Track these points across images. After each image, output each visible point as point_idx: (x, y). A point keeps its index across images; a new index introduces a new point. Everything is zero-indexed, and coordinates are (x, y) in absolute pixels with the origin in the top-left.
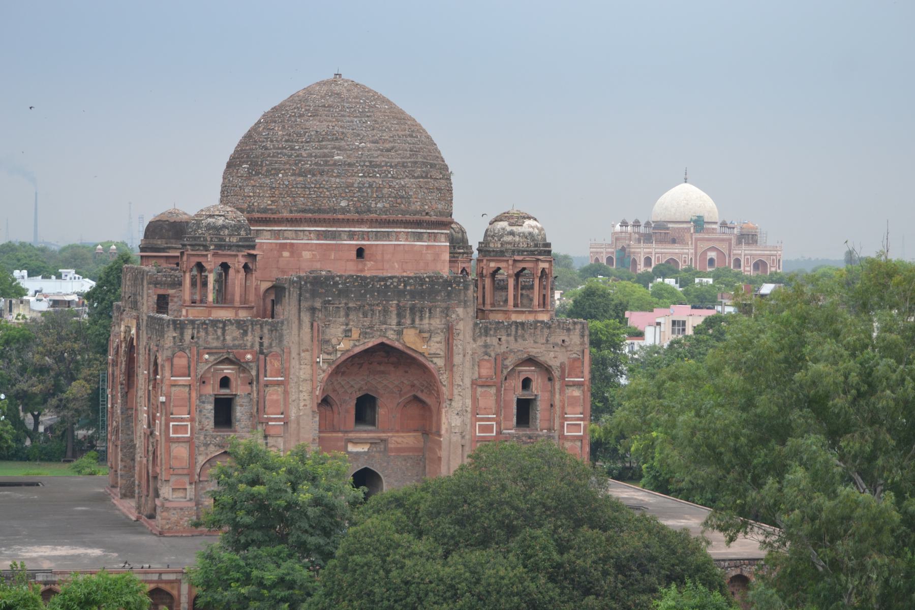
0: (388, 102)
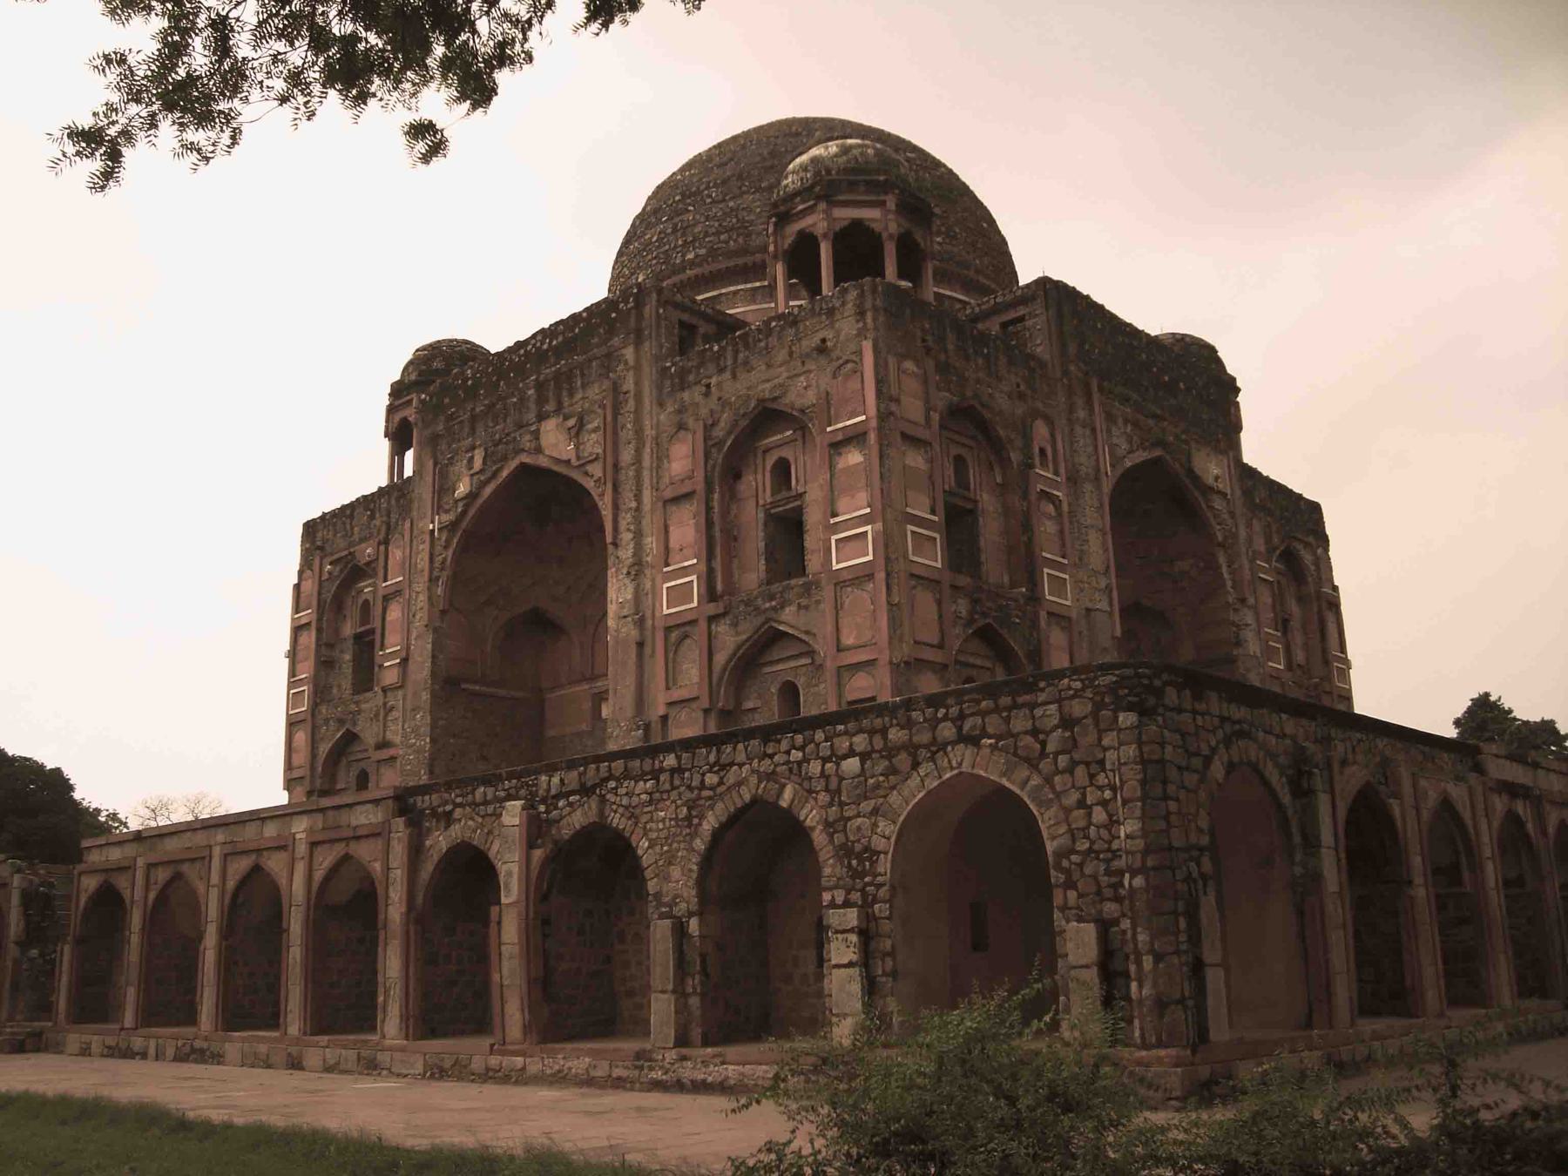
0: (915, 149)
